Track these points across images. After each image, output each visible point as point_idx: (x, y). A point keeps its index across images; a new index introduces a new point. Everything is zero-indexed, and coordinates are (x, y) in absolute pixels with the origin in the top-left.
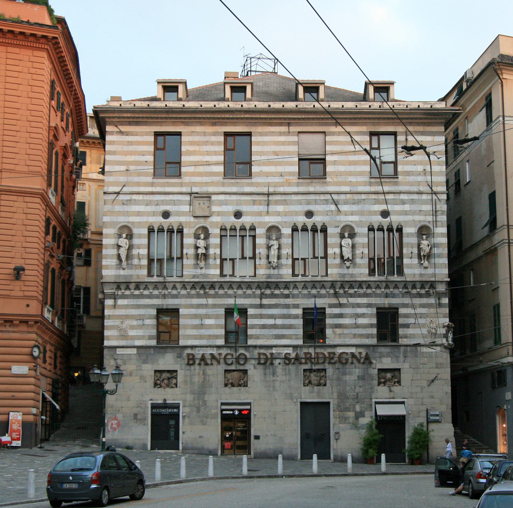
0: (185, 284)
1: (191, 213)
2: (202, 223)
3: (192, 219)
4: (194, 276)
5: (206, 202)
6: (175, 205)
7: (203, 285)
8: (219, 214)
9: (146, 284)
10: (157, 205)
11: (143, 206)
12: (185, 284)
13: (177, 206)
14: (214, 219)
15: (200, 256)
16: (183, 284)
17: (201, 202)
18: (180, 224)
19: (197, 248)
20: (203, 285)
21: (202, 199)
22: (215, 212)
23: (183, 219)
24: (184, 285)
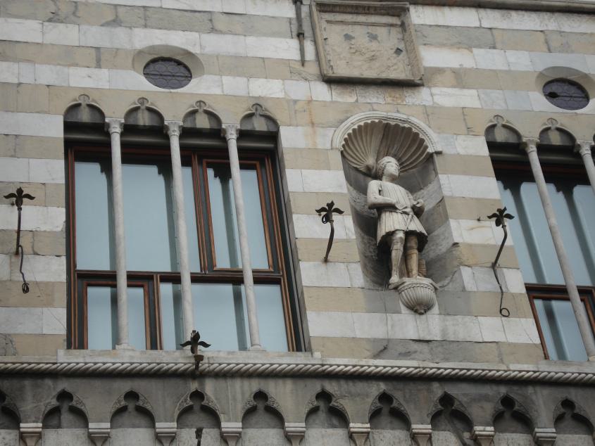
0: (331, 387)
1: (312, 69)
2: (379, 106)
3: (322, 92)
4: (383, 349)
5: (381, 32)
6: (213, 30)
7: (446, 400)
8: (460, 78)
9: (64, 385)
10: (116, 22)
11: (34, 25)
12: (331, 387)
13: (229, 37)
14: (441, 96)
15: (397, 252)
16: (317, 386)
17: (360, 33)
18: (257, 109)
19: (368, 220)
20: (446, 400)
21: (361, 18)
22: (439, 71)
23: (269, 89)
24: (324, 396)
